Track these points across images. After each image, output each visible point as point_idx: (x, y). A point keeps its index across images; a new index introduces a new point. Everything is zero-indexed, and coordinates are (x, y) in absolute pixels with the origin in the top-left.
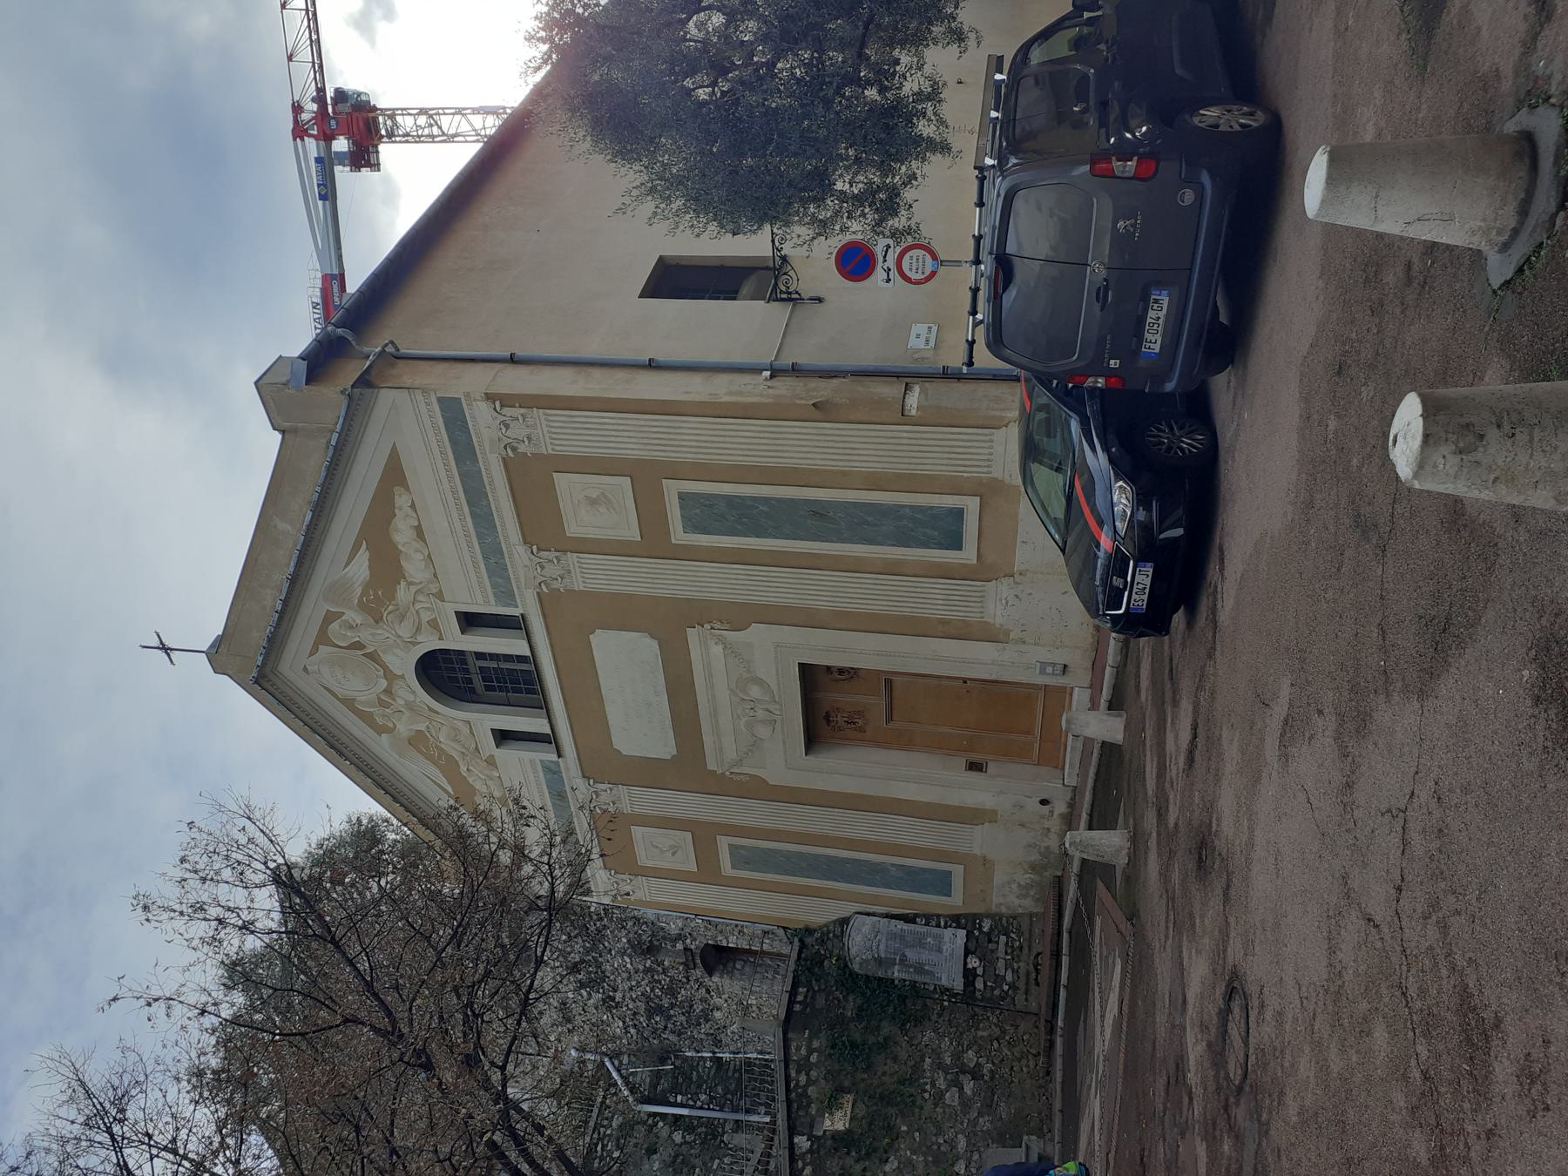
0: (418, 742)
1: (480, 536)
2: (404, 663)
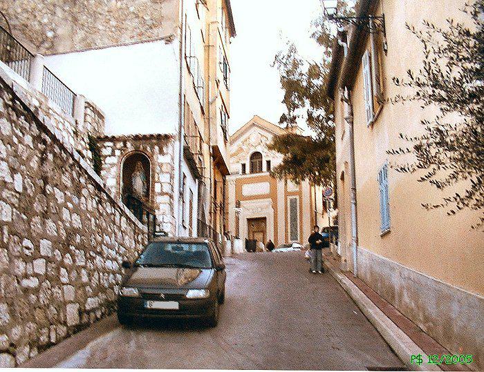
0: (241, 149)
2: (259, 149)
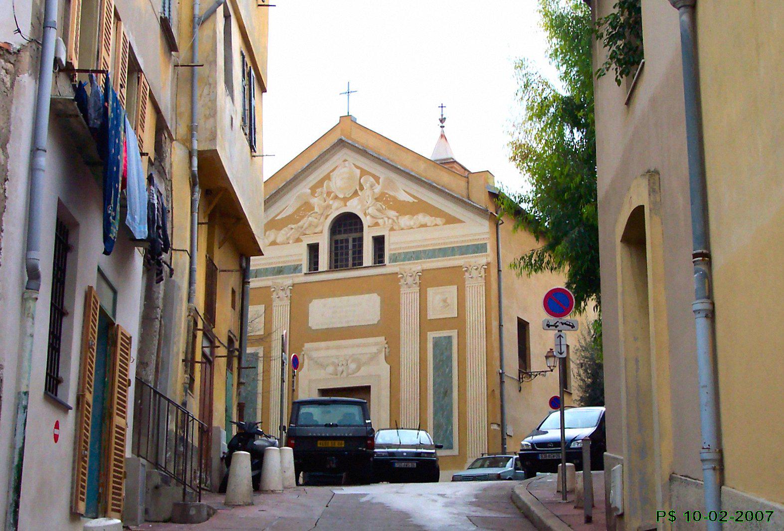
0: (306, 207)
1: (425, 251)
2: (353, 207)
